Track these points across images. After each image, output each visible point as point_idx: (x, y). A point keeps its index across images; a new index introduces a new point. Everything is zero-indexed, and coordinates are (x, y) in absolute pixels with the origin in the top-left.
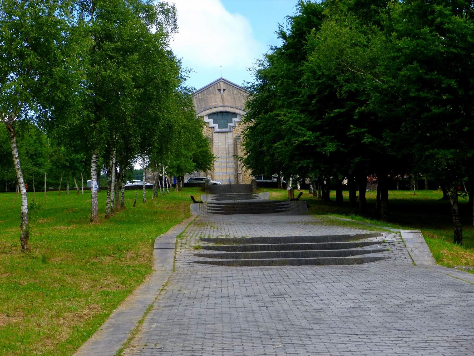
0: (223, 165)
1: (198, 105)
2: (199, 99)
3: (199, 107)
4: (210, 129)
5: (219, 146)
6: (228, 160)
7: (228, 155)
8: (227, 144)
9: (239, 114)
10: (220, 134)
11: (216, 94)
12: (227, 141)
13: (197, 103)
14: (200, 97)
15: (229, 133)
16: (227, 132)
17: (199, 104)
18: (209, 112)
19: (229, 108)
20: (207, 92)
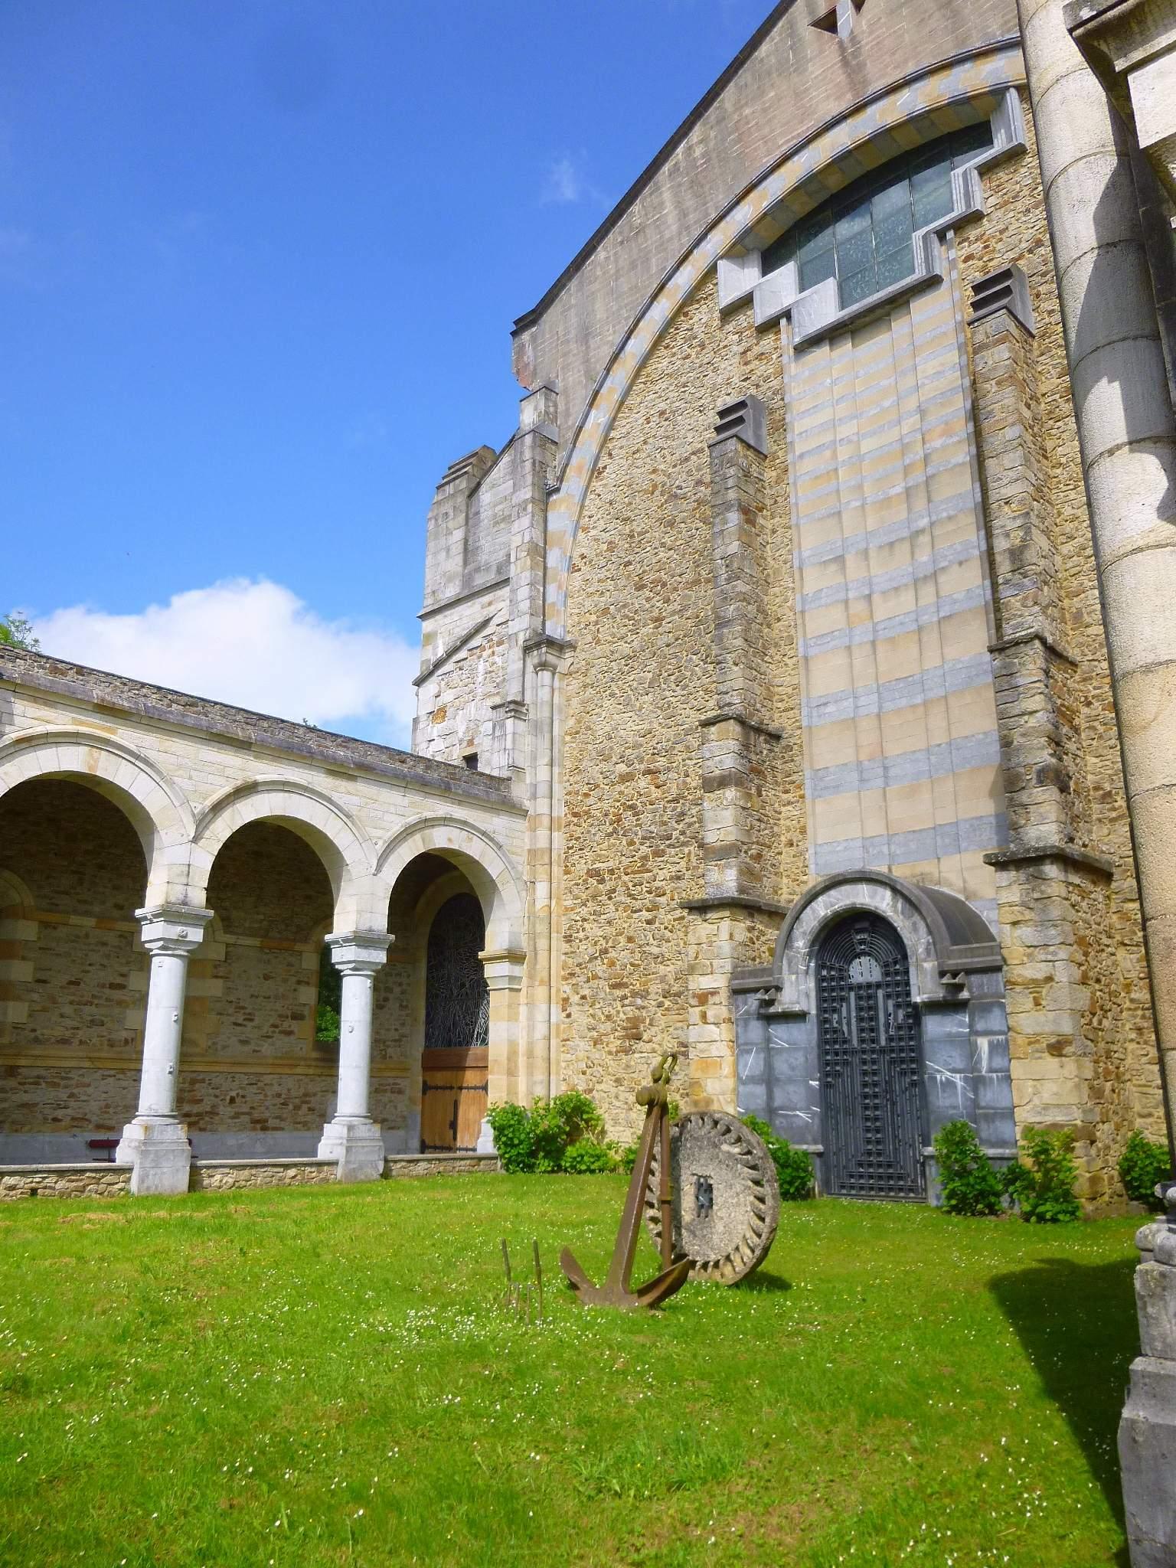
0: (883, 610)
1: (683, 214)
2: (692, 164)
3: (692, 217)
4: (768, 342)
5: (844, 452)
6: (924, 557)
7: (920, 503)
8: (912, 404)
9: (998, 93)
10: (846, 347)
11: (800, 68)
12: (909, 382)
13: (678, 204)
14: (698, 151)
15: (920, 307)
16: (899, 302)
17: (690, 202)
18: (745, 214)
19: (905, 94)
20: (740, 89)
